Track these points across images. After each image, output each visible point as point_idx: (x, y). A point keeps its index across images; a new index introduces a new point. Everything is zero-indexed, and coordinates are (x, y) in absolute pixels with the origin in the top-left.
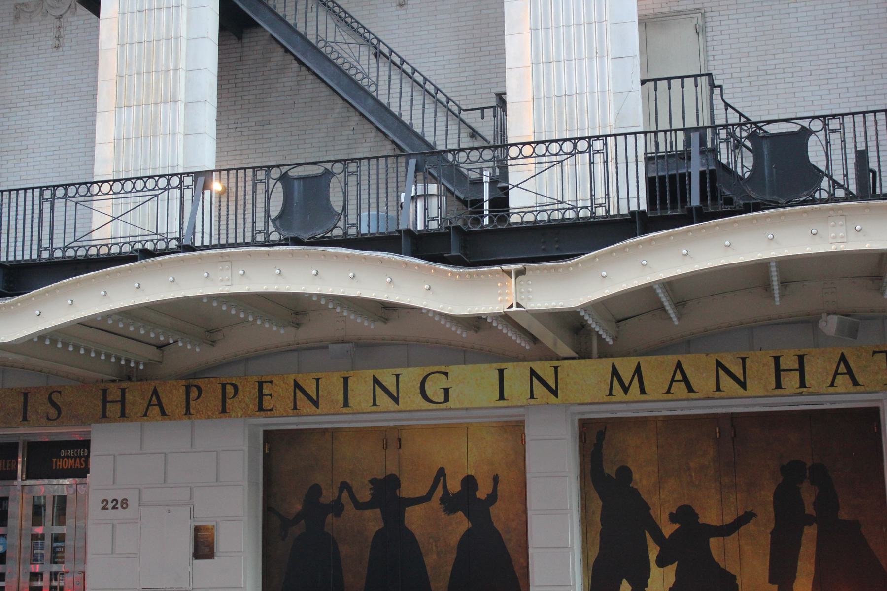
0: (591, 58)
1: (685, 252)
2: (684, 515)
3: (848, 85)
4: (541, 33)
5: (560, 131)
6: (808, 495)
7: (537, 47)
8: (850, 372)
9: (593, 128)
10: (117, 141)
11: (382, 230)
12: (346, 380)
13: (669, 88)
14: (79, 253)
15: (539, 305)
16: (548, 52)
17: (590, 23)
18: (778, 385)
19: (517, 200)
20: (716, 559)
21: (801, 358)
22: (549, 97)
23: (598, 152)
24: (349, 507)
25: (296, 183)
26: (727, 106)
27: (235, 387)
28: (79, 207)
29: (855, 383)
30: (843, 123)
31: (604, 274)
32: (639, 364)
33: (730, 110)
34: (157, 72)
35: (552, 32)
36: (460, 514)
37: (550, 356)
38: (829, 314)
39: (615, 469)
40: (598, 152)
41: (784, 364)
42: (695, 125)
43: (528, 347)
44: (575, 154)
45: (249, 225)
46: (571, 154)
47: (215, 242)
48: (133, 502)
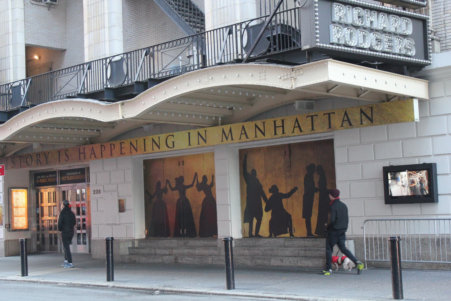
2: (274, 189)
6: (316, 179)
8: (299, 127)
10: (89, 46)
11: (143, 80)
12: (145, 140)
18: (275, 134)
20: (285, 208)
24: (169, 190)
25: (114, 64)
27: (114, 144)
29: (301, 131)
34: (99, 16)
36: (202, 191)
39: (251, 170)
45: (149, 72)
48: (102, 191)
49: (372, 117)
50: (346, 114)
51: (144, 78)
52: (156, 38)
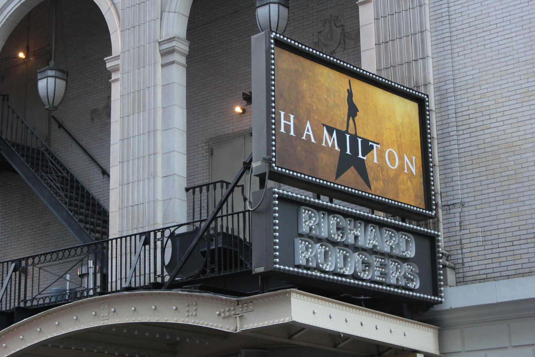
0: (149, 179)
4: (125, 164)
14: (40, 303)
28: (41, 271)
45: (17, 297)
47: (138, 285)
51: (8, 305)
52: (33, 245)
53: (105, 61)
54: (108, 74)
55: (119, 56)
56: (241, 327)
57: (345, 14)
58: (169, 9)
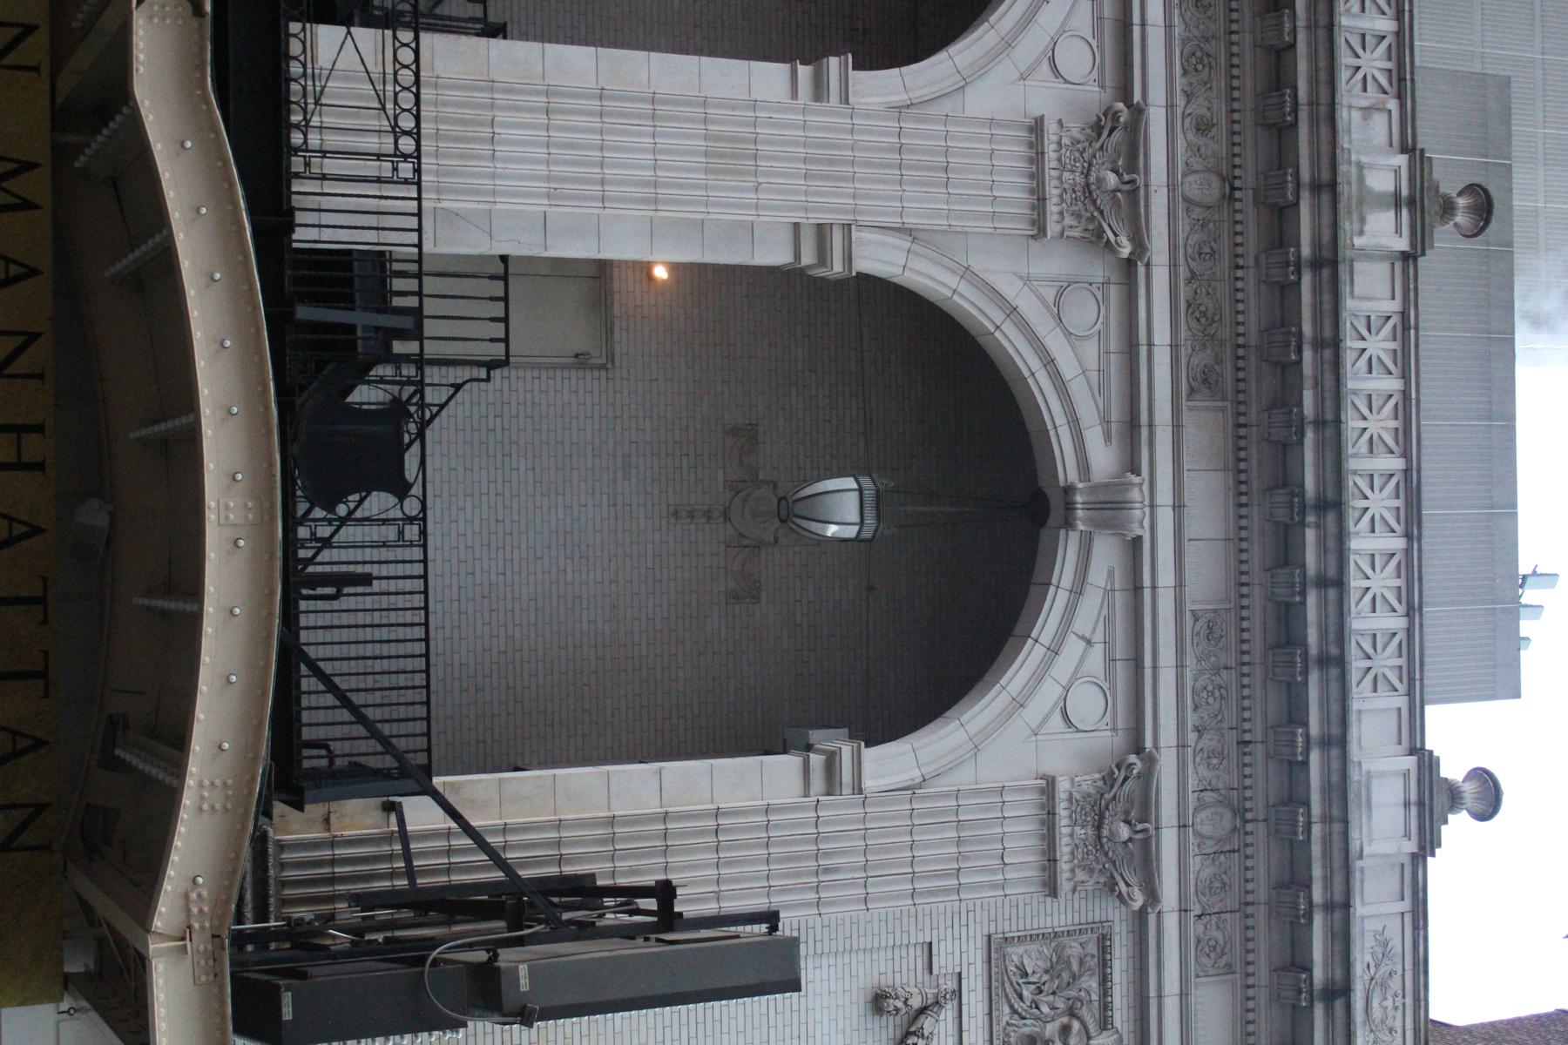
0: (548, 179)
1: (217, 276)
3: (478, 576)
4: (594, 104)
5: (436, 120)
7: (576, 96)
9: (437, 173)
13: (491, 299)
15: (141, 33)
16: (563, 112)
17: (603, 182)
19: (328, 37)
21: (39, 466)
22: (492, 107)
23: (395, 169)
26: (458, 387)
30: (412, 545)
31: (189, 144)
32: (37, 207)
33: (452, 391)
35: (594, 122)
37: (59, 56)
38: (111, 513)
40: (395, 169)
41: (30, 440)
42: (427, 333)
43: (74, 25)
44: (394, 132)
46: (396, 132)
49: (17, 850)
50: (39, 744)
53: (845, 53)
54: (813, 56)
55: (847, 102)
56: (161, 953)
57: (797, 549)
58: (916, 253)
